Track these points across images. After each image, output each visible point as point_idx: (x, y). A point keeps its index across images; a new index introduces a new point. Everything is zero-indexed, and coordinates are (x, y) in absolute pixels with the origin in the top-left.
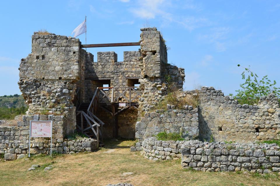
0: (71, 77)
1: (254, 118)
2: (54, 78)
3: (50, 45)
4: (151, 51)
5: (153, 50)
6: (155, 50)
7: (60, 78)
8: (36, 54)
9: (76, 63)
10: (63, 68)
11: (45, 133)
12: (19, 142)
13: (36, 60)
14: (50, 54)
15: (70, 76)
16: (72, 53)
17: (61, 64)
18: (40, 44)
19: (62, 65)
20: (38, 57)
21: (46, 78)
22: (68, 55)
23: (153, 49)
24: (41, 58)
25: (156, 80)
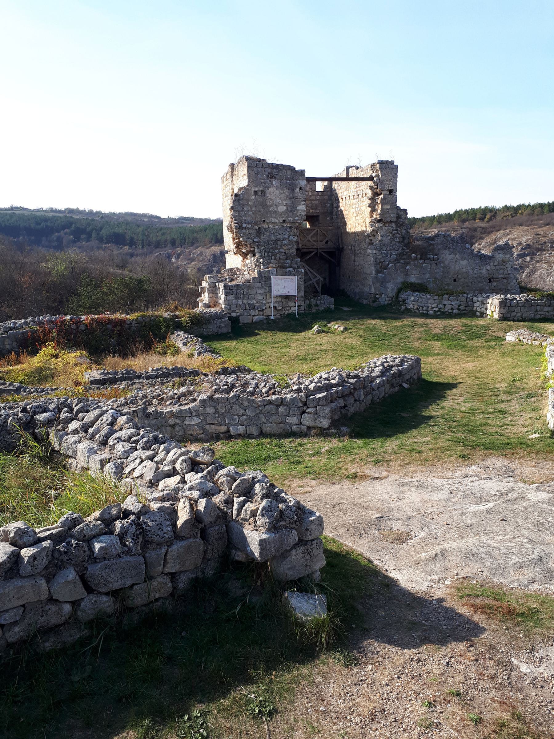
0: (297, 220)
1: (489, 268)
2: (277, 221)
3: (271, 177)
4: (387, 190)
5: (390, 188)
6: (392, 188)
7: (284, 221)
8: (253, 190)
9: (303, 203)
10: (287, 208)
11: (289, 290)
12: (255, 302)
13: (253, 197)
14: (271, 190)
15: (297, 218)
16: (298, 190)
17: (285, 202)
18: (258, 175)
19: (286, 205)
20: (256, 193)
21: (267, 221)
22: (293, 191)
23: (391, 187)
24: (260, 193)
25: (390, 225)
